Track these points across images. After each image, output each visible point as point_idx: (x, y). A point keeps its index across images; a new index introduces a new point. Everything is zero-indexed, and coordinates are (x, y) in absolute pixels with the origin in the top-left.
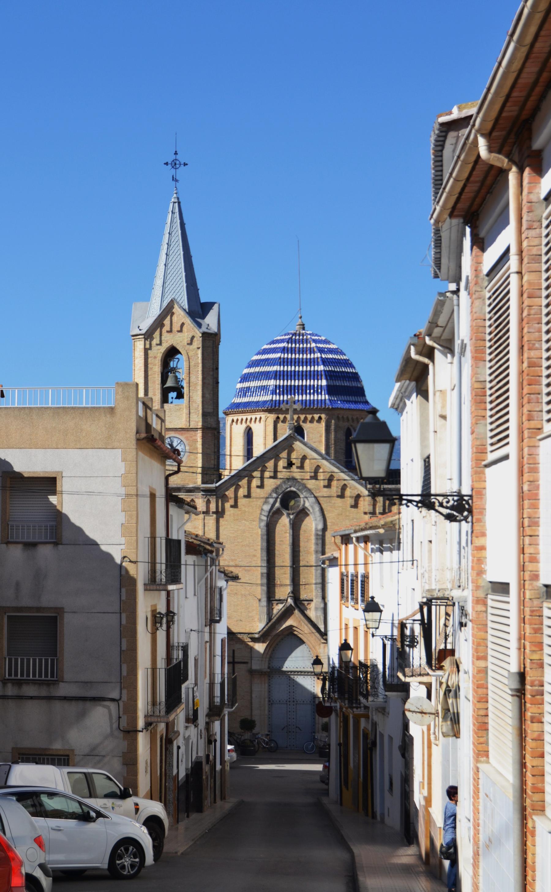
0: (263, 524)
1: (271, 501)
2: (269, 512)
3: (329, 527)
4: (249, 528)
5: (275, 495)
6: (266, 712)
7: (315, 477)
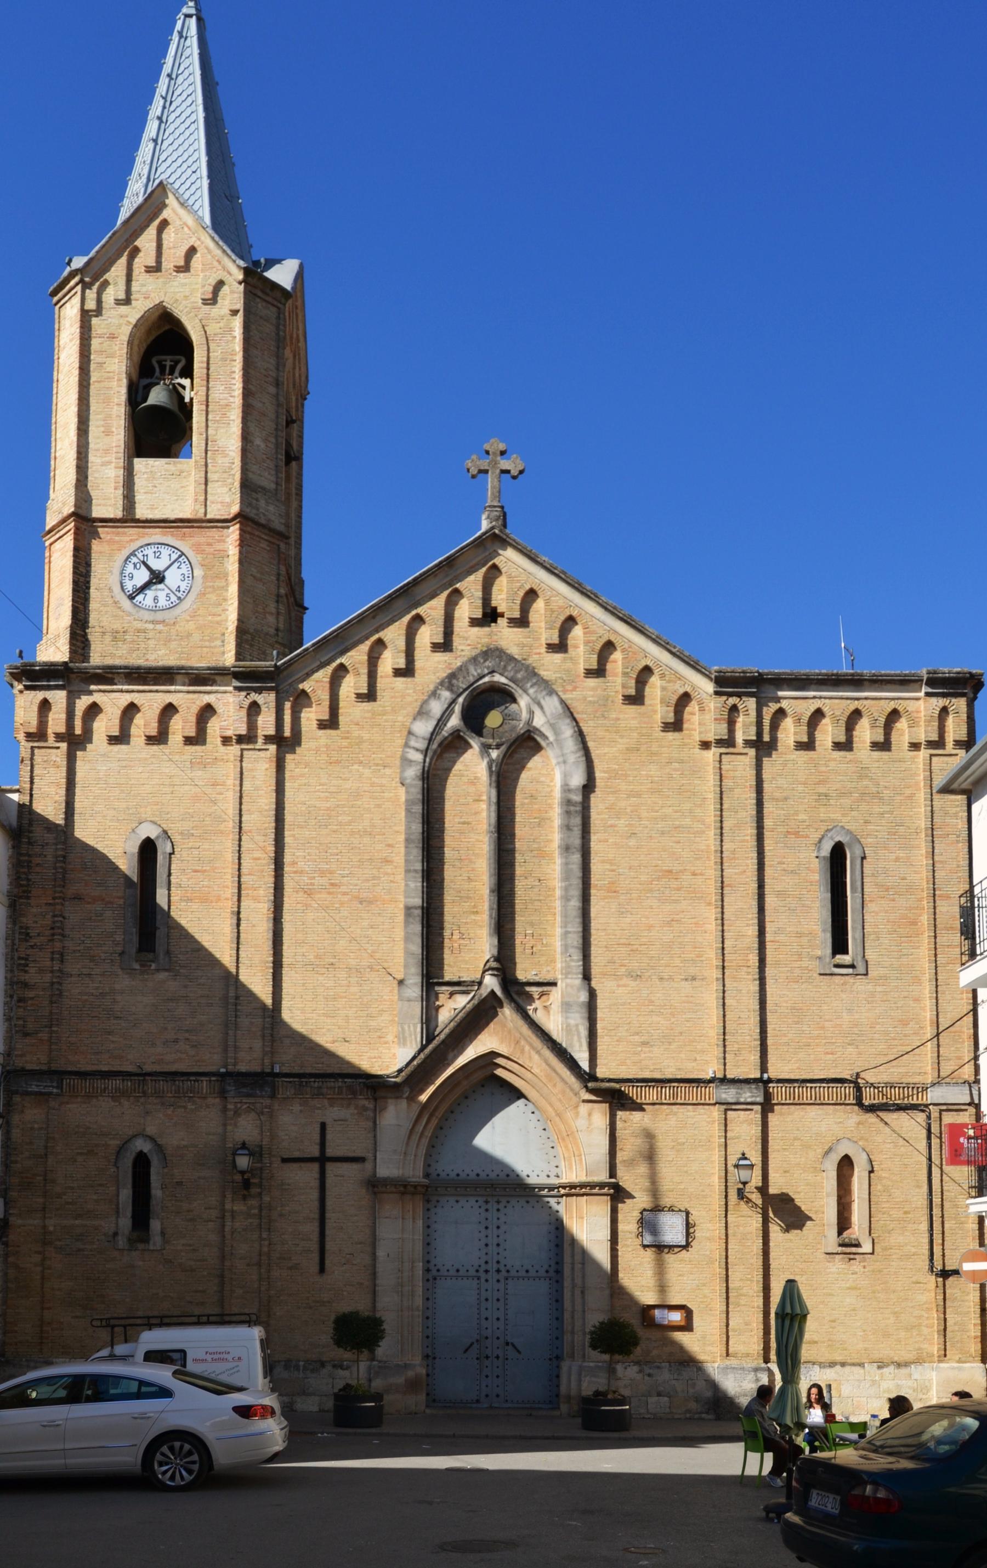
0: (413, 773)
1: (437, 708)
2: (430, 740)
3: (599, 782)
4: (373, 785)
5: (446, 695)
7: (560, 647)
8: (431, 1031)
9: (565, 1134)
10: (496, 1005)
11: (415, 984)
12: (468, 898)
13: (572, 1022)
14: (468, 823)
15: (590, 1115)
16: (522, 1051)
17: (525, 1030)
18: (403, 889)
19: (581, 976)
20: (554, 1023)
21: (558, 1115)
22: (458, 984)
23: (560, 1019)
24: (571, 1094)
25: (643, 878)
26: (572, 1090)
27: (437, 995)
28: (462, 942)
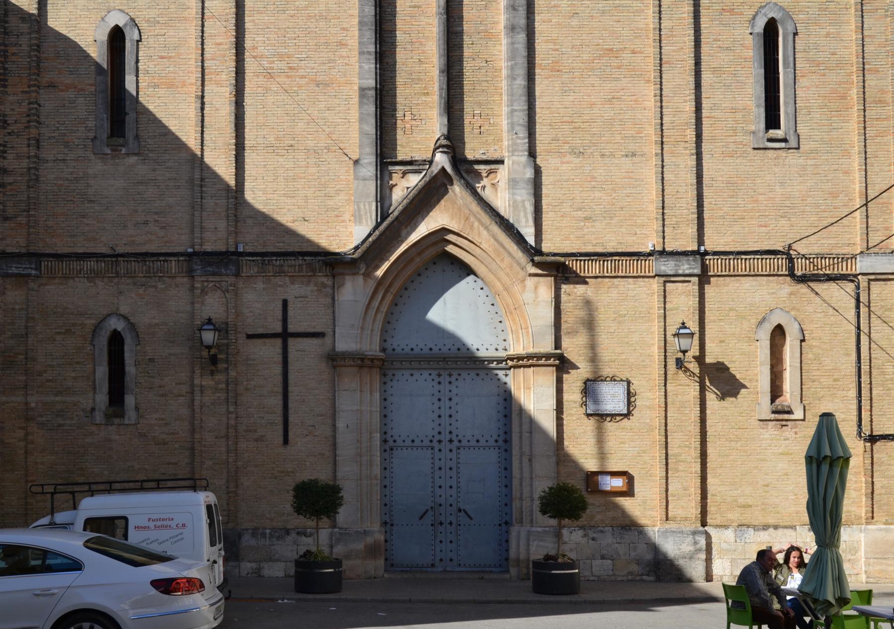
6: (377, 470)
8: (385, 209)
9: (512, 308)
10: (446, 182)
11: (370, 163)
12: (419, 79)
13: (519, 198)
14: (419, 7)
15: (536, 288)
16: (472, 227)
17: (475, 207)
18: (359, 71)
19: (527, 153)
20: (501, 200)
22: (410, 163)
24: (518, 268)
25: (585, 57)
26: (519, 264)
27: (391, 173)
28: (414, 122)
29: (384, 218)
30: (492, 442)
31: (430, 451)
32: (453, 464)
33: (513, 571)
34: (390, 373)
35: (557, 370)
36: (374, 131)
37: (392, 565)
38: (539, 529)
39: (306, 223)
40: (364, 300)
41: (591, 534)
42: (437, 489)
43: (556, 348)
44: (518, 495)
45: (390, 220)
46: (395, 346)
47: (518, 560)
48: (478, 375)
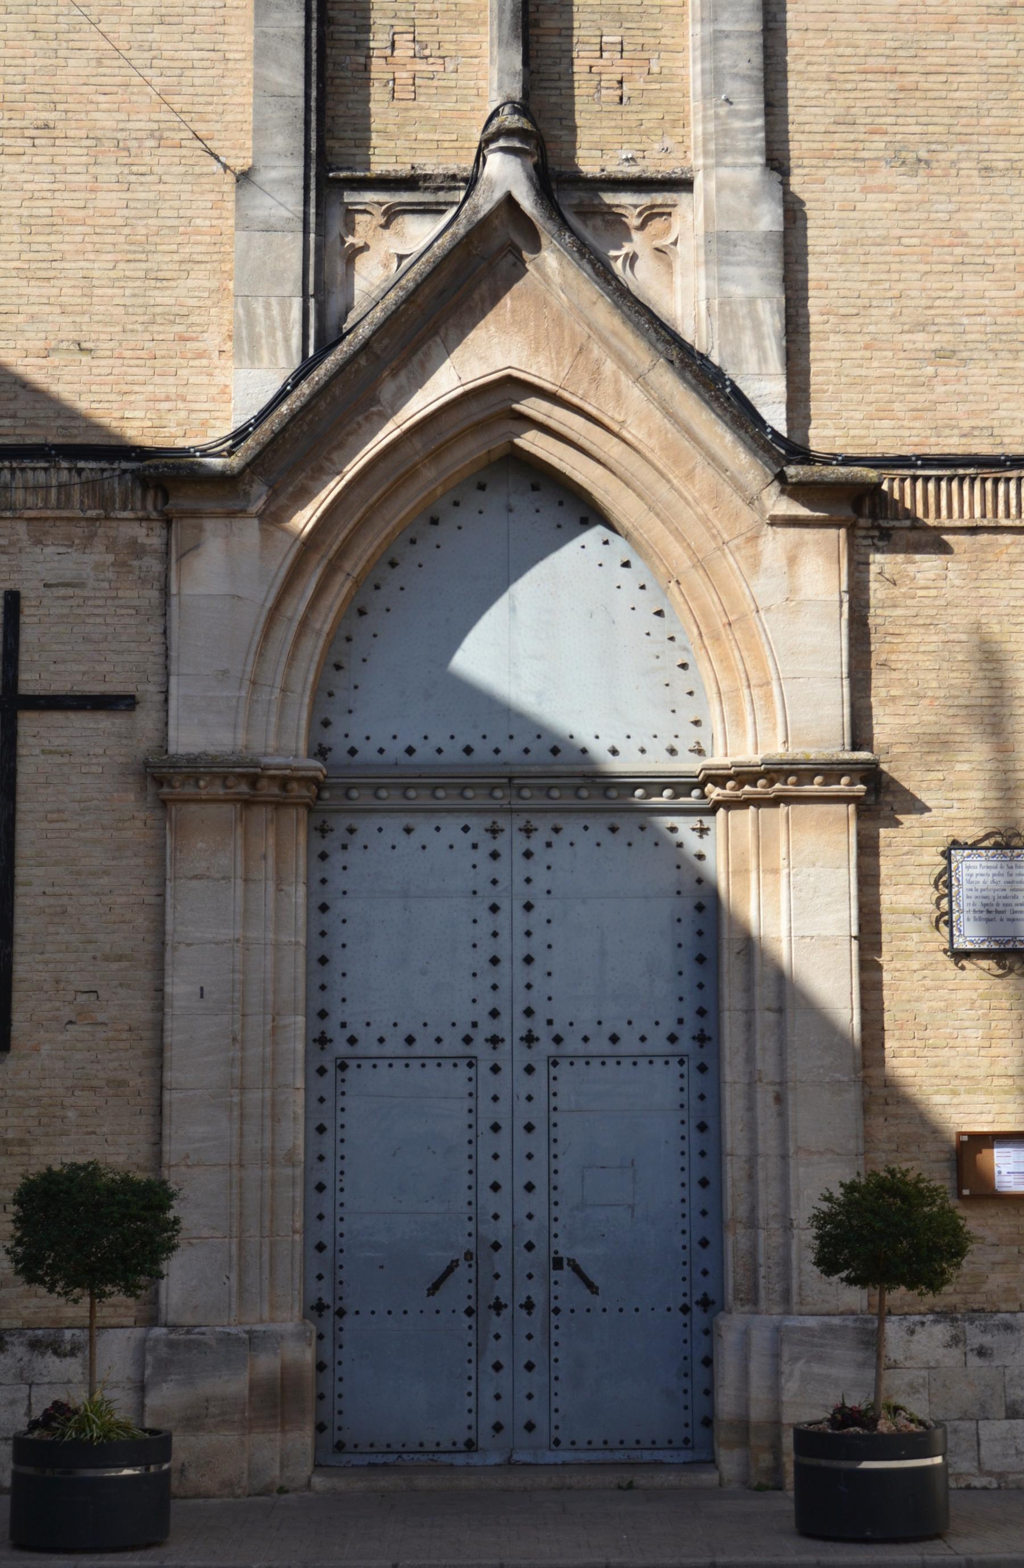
6: (294, 1135)
8: (331, 321)
9: (720, 621)
10: (519, 241)
11: (287, 181)
13: (737, 291)
15: (792, 561)
16: (596, 376)
17: (604, 315)
19: (760, 160)
20: (684, 298)
21: (701, 564)
22: (410, 182)
23: (702, 284)
24: (738, 502)
26: (739, 488)
27: (350, 214)
28: (420, 66)
29: (325, 348)
30: (658, 1043)
31: (464, 1071)
32: (537, 1114)
33: (730, 1461)
34: (340, 823)
35: (860, 815)
36: (300, 86)
37: (340, 1447)
38: (812, 1322)
39: (85, 358)
40: (264, 595)
41: (976, 1338)
42: (485, 1194)
43: (855, 747)
44: (742, 1211)
45: (344, 350)
46: (356, 741)
47: (743, 1426)
48: (613, 830)
